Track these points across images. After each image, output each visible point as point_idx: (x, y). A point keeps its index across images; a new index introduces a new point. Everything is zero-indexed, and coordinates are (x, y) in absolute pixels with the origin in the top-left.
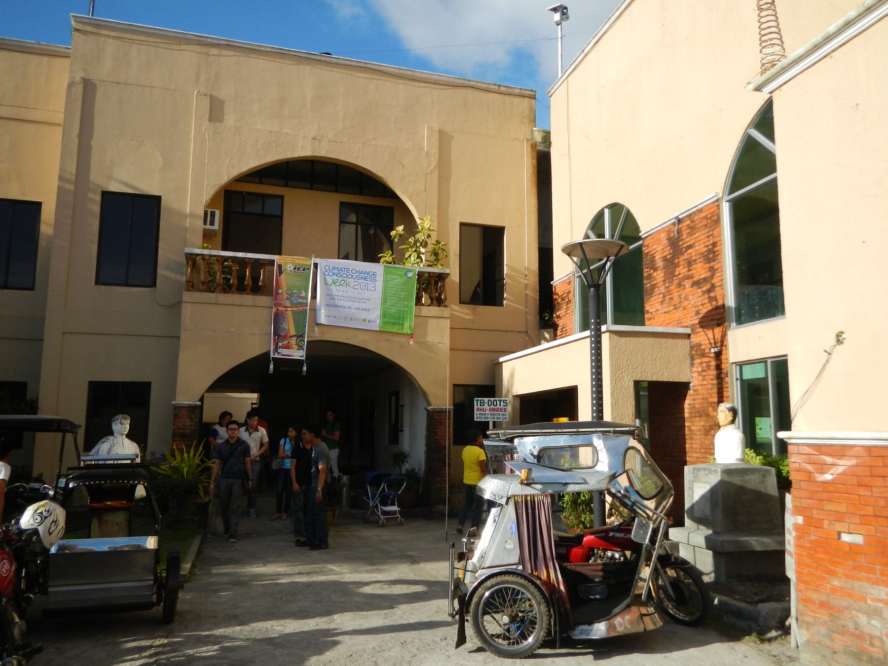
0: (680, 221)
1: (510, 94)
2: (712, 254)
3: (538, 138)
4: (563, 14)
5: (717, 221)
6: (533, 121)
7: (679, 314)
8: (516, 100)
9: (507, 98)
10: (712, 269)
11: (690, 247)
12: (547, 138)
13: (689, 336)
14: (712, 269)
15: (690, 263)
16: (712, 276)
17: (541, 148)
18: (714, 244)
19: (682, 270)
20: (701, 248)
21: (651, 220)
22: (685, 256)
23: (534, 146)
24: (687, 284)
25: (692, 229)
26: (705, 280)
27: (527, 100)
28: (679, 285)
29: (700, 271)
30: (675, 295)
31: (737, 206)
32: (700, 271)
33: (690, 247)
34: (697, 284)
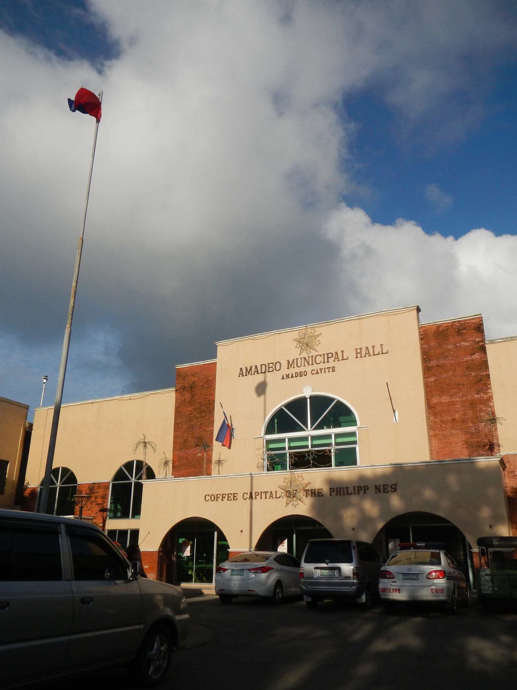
0: (94, 483)
1: (20, 406)
2: (105, 497)
3: (27, 425)
4: (47, 380)
5: (108, 488)
6: (26, 418)
7: (89, 512)
8: (22, 409)
9: (19, 407)
10: (104, 501)
11: (97, 493)
12: (31, 425)
13: (92, 519)
14: (104, 501)
15: (96, 498)
16: (104, 504)
17: (27, 430)
18: (106, 494)
19: (93, 499)
20: (101, 494)
21: (83, 478)
22: (95, 495)
23: (25, 429)
24: (94, 504)
25: (99, 488)
26: (101, 504)
27: (25, 409)
28: (91, 503)
29: (100, 501)
30: (89, 507)
31: (113, 485)
32: (100, 501)
33: (97, 493)
34: (98, 504)
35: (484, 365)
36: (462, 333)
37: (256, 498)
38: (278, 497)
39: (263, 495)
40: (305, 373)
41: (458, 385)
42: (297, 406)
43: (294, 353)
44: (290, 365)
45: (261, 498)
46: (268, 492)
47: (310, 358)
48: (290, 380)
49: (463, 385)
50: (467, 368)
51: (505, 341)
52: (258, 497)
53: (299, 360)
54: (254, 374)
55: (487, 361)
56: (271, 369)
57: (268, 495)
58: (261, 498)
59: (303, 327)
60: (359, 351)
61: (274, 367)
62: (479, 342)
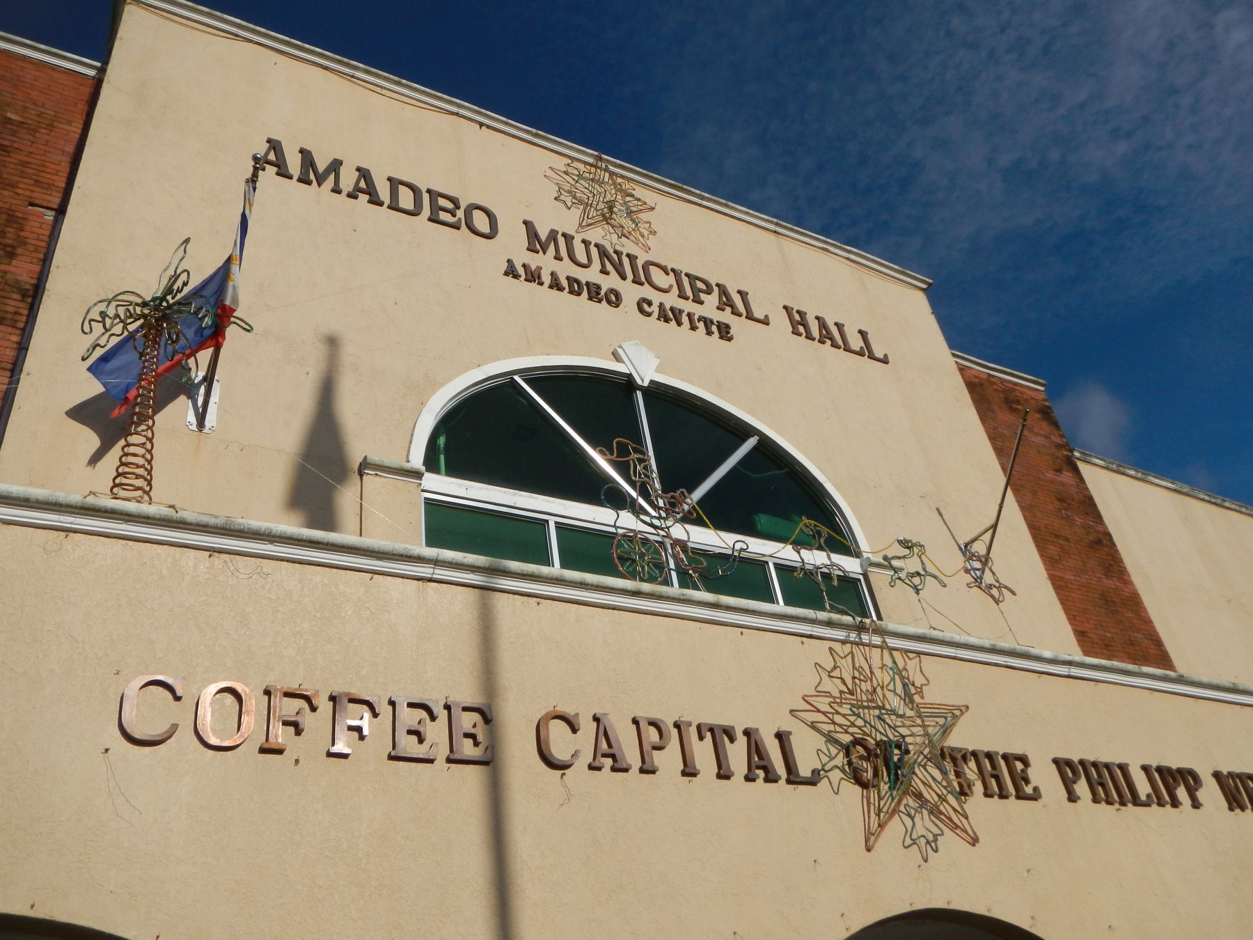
35: (1088, 506)
36: (1016, 410)
37: (647, 770)
38: (804, 771)
39: (703, 752)
40: (614, 299)
41: (1057, 536)
42: (600, 398)
43: (557, 218)
44: (535, 242)
45: (689, 771)
46: (729, 733)
47: (626, 261)
48: (543, 293)
49: (1067, 540)
50: (1059, 500)
51: (1107, 468)
52: (669, 760)
53: (577, 244)
54: (352, 196)
55: (1091, 498)
56: (444, 216)
57: (737, 754)
58: (689, 771)
59: (588, 155)
60: (797, 317)
61: (460, 214)
62: (1059, 446)
